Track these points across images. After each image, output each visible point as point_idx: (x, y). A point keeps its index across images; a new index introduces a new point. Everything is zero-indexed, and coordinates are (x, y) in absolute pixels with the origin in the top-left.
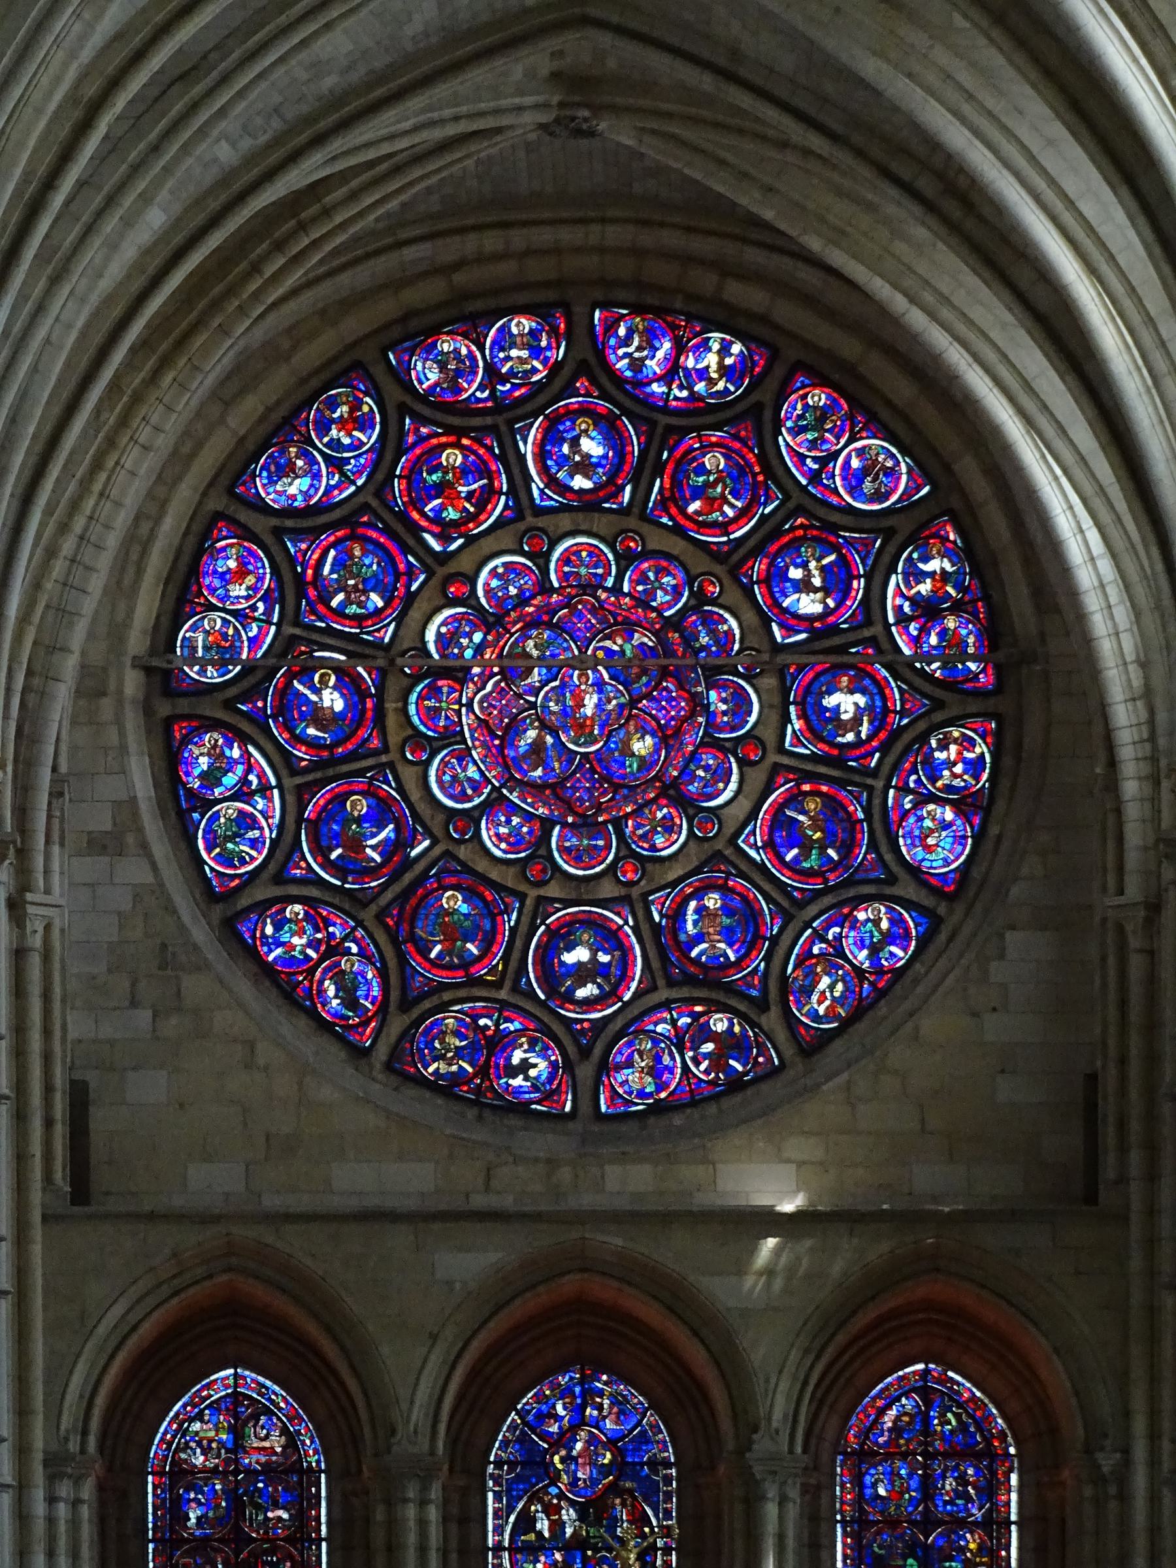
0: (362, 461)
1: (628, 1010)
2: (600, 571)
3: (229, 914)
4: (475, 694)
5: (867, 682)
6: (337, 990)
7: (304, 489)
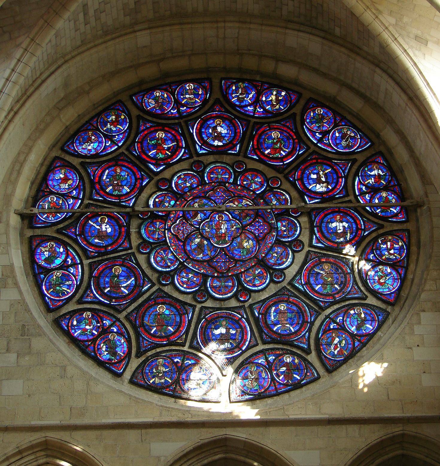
0: (121, 136)
1: (244, 354)
2: (227, 176)
3: (56, 317)
4: (172, 225)
5: (348, 218)
6: (106, 348)
7: (95, 147)
